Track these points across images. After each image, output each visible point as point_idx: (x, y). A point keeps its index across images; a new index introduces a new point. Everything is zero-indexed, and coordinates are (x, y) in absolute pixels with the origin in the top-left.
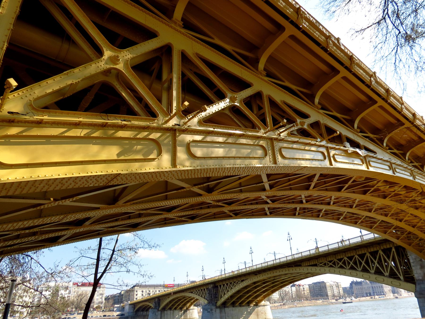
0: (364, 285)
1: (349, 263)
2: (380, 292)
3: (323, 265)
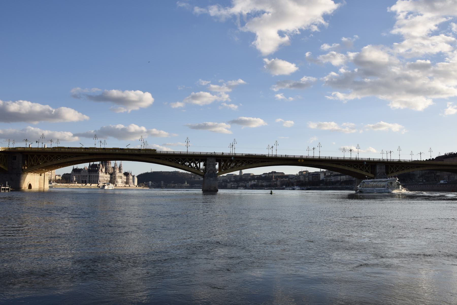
0: (82, 173)
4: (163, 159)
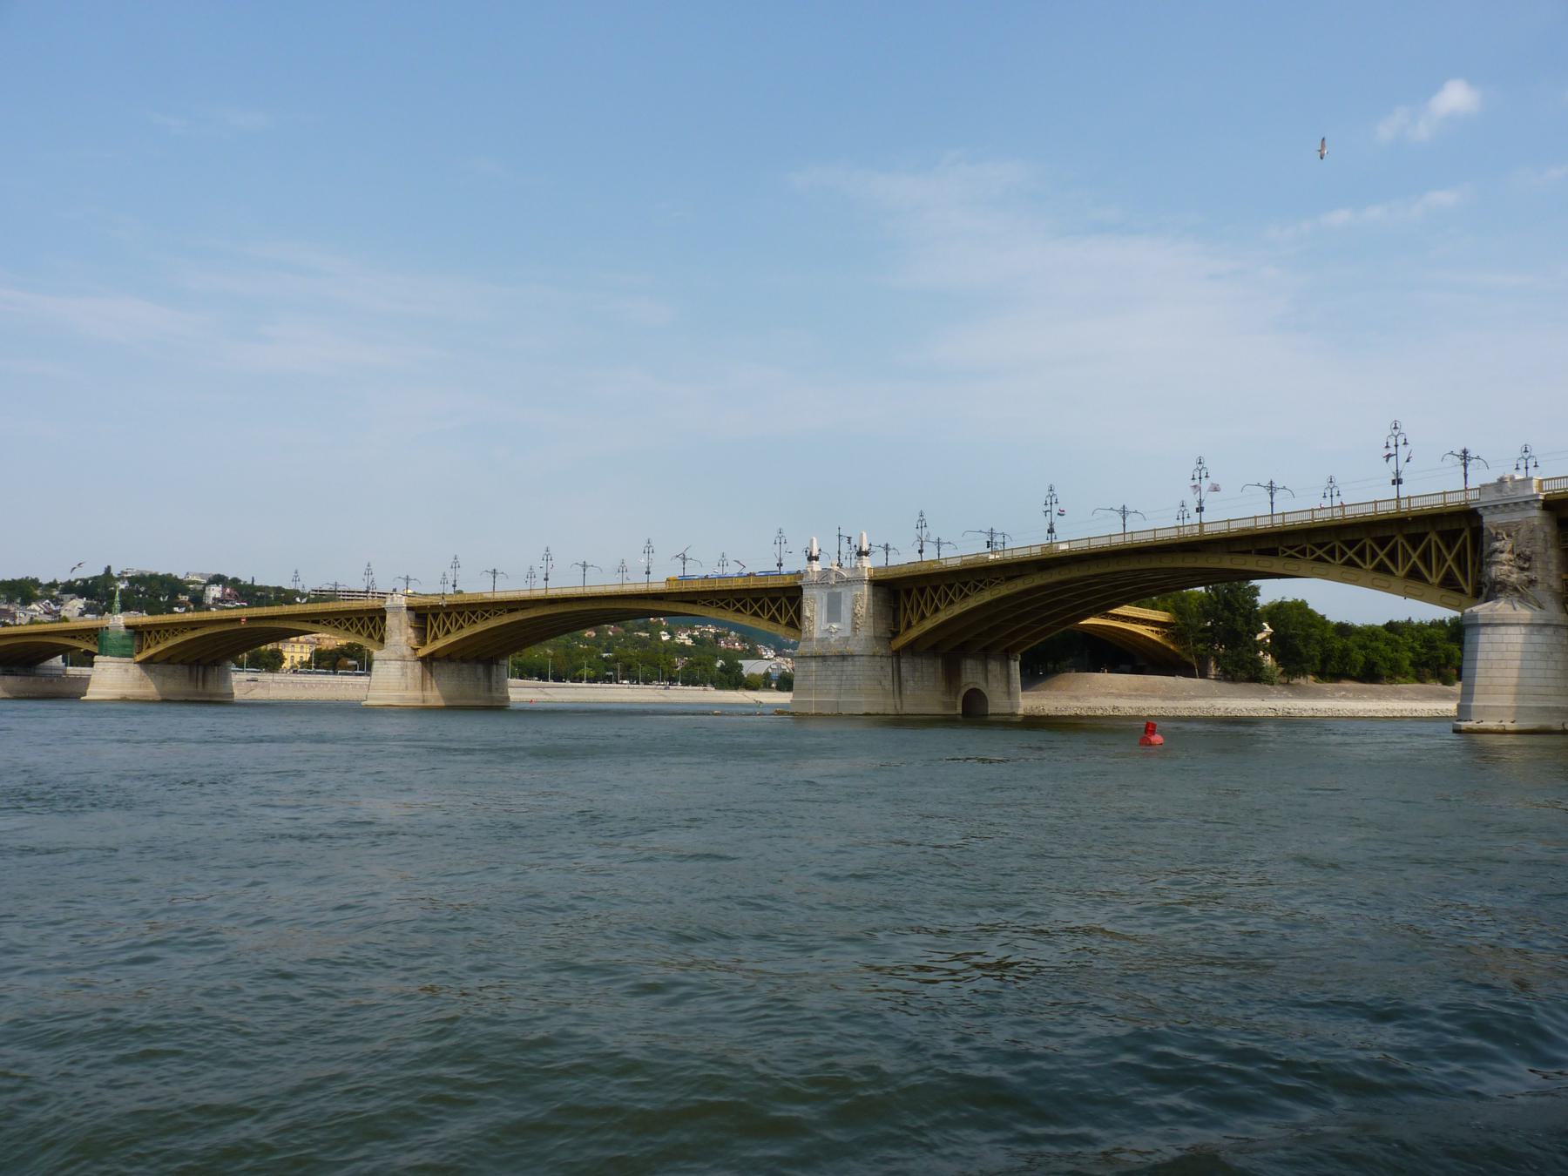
4: (1289, 552)
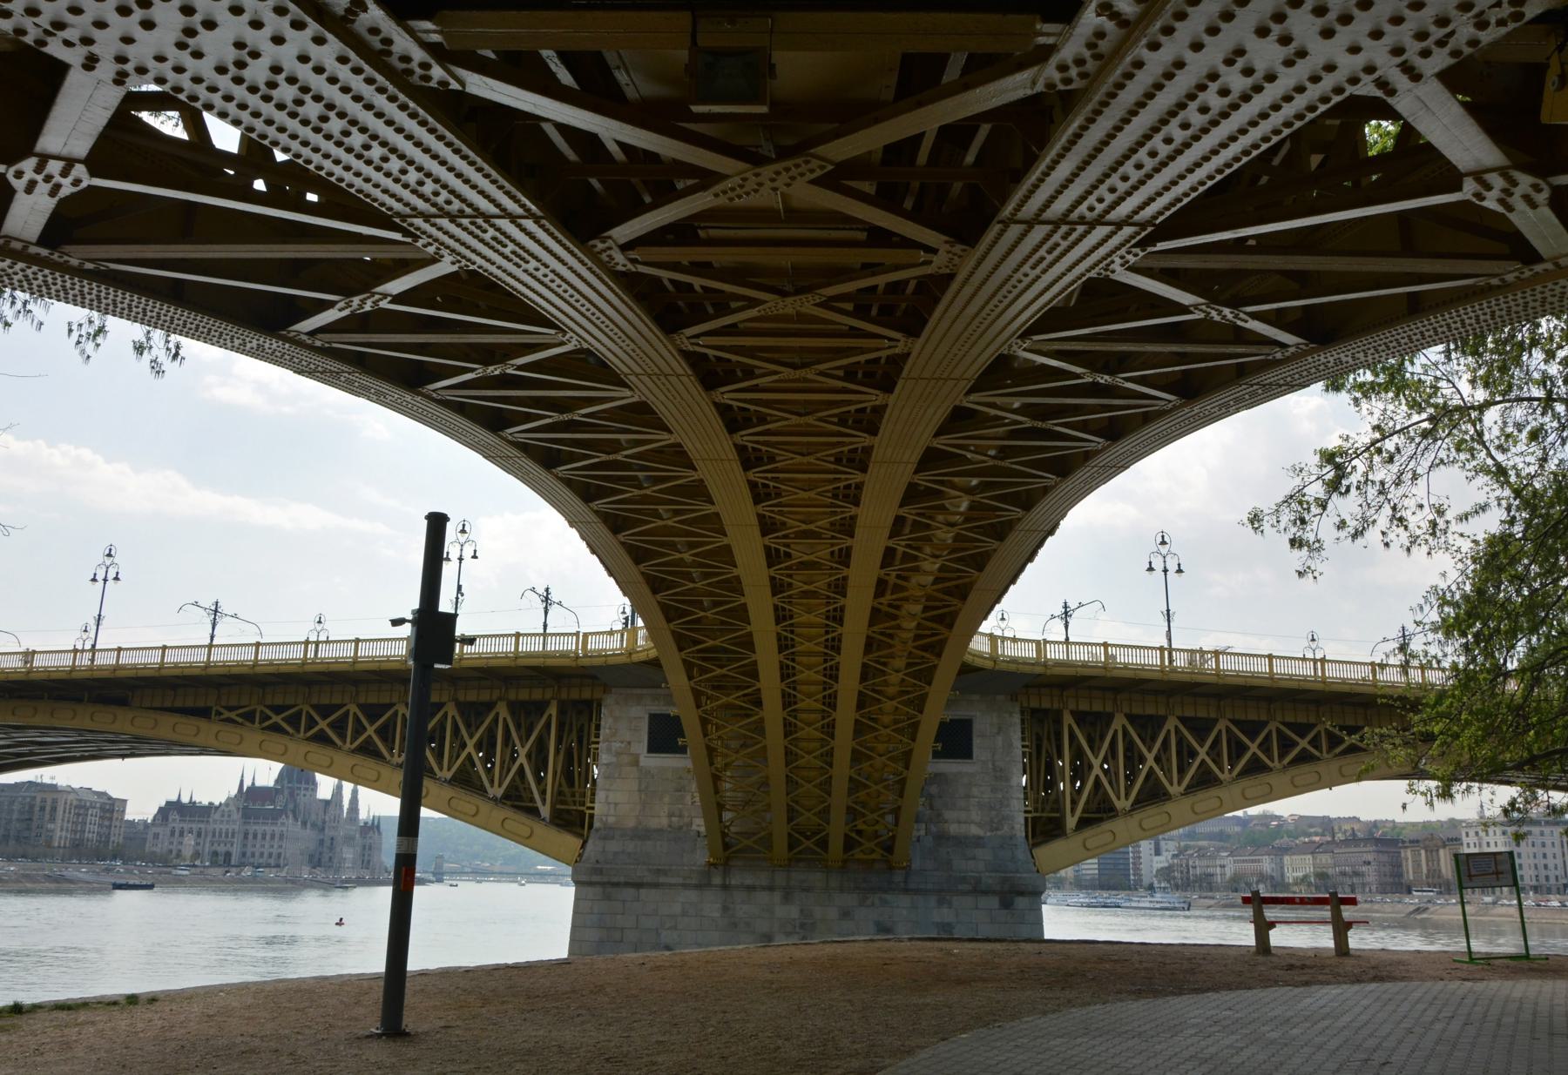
0: (215, 821)
1: (360, 729)
2: (266, 855)
3: (240, 720)
